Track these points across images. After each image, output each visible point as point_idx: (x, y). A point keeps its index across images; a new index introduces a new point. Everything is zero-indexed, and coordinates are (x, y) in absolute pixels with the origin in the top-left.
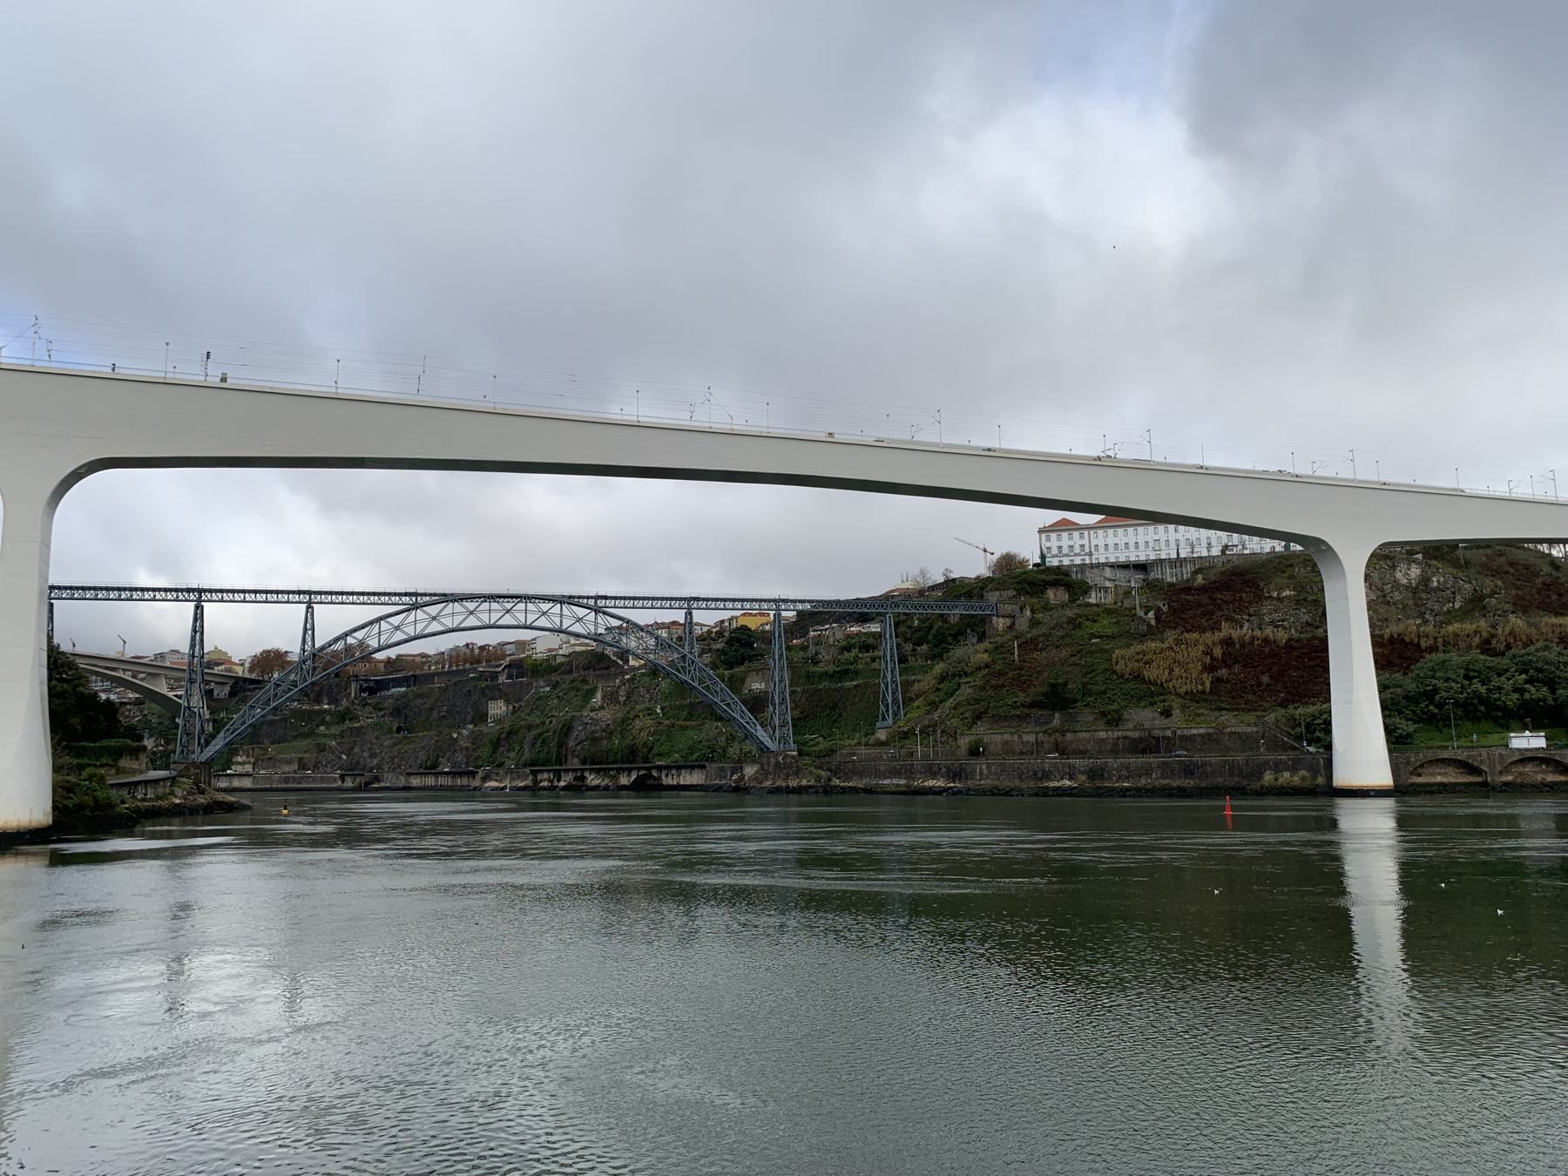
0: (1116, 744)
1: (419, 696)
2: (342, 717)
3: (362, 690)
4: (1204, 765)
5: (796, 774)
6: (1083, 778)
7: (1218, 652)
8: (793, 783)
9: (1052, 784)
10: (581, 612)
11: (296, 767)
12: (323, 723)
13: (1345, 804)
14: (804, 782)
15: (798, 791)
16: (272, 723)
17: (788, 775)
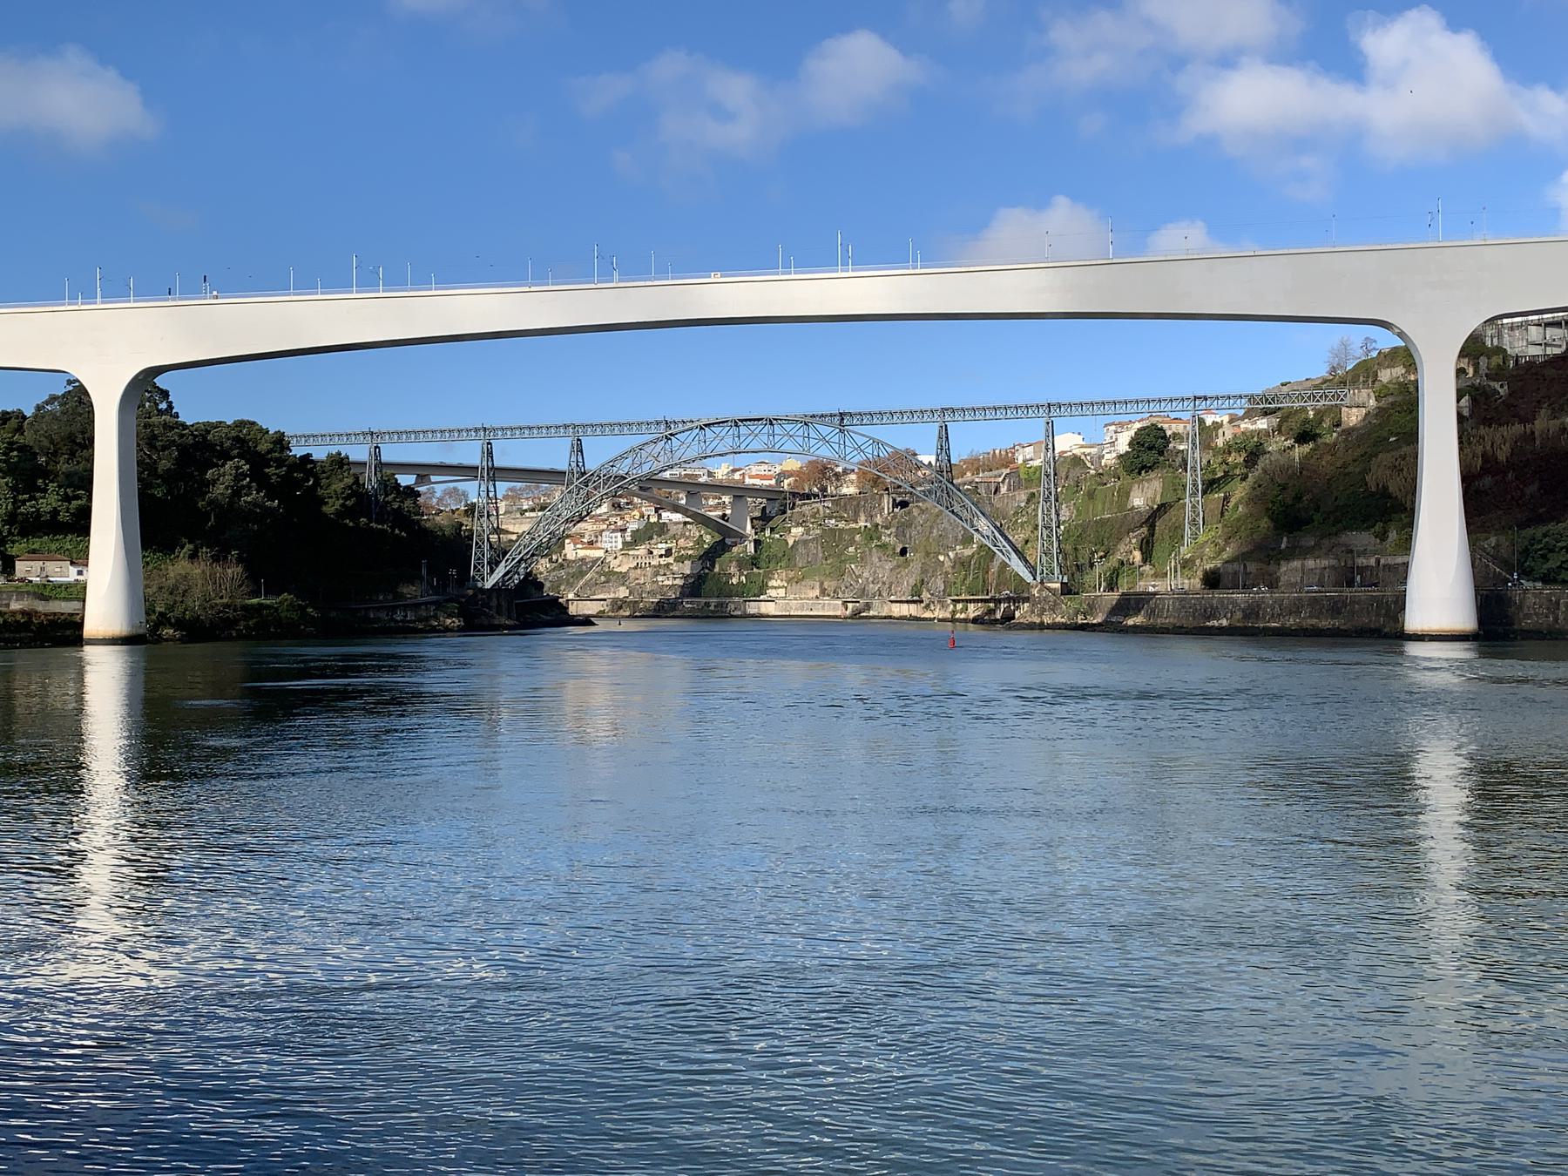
0: (1322, 575)
1: (923, 511)
2: (872, 533)
3: (895, 505)
4: (1353, 602)
5: (1053, 610)
6: (1239, 615)
7: (1502, 456)
8: (1047, 620)
9: (1216, 623)
10: (824, 430)
11: (817, 592)
12: (852, 542)
13: (1414, 649)
14: (1059, 619)
15: (1055, 627)
16: (805, 542)
17: (1043, 611)
